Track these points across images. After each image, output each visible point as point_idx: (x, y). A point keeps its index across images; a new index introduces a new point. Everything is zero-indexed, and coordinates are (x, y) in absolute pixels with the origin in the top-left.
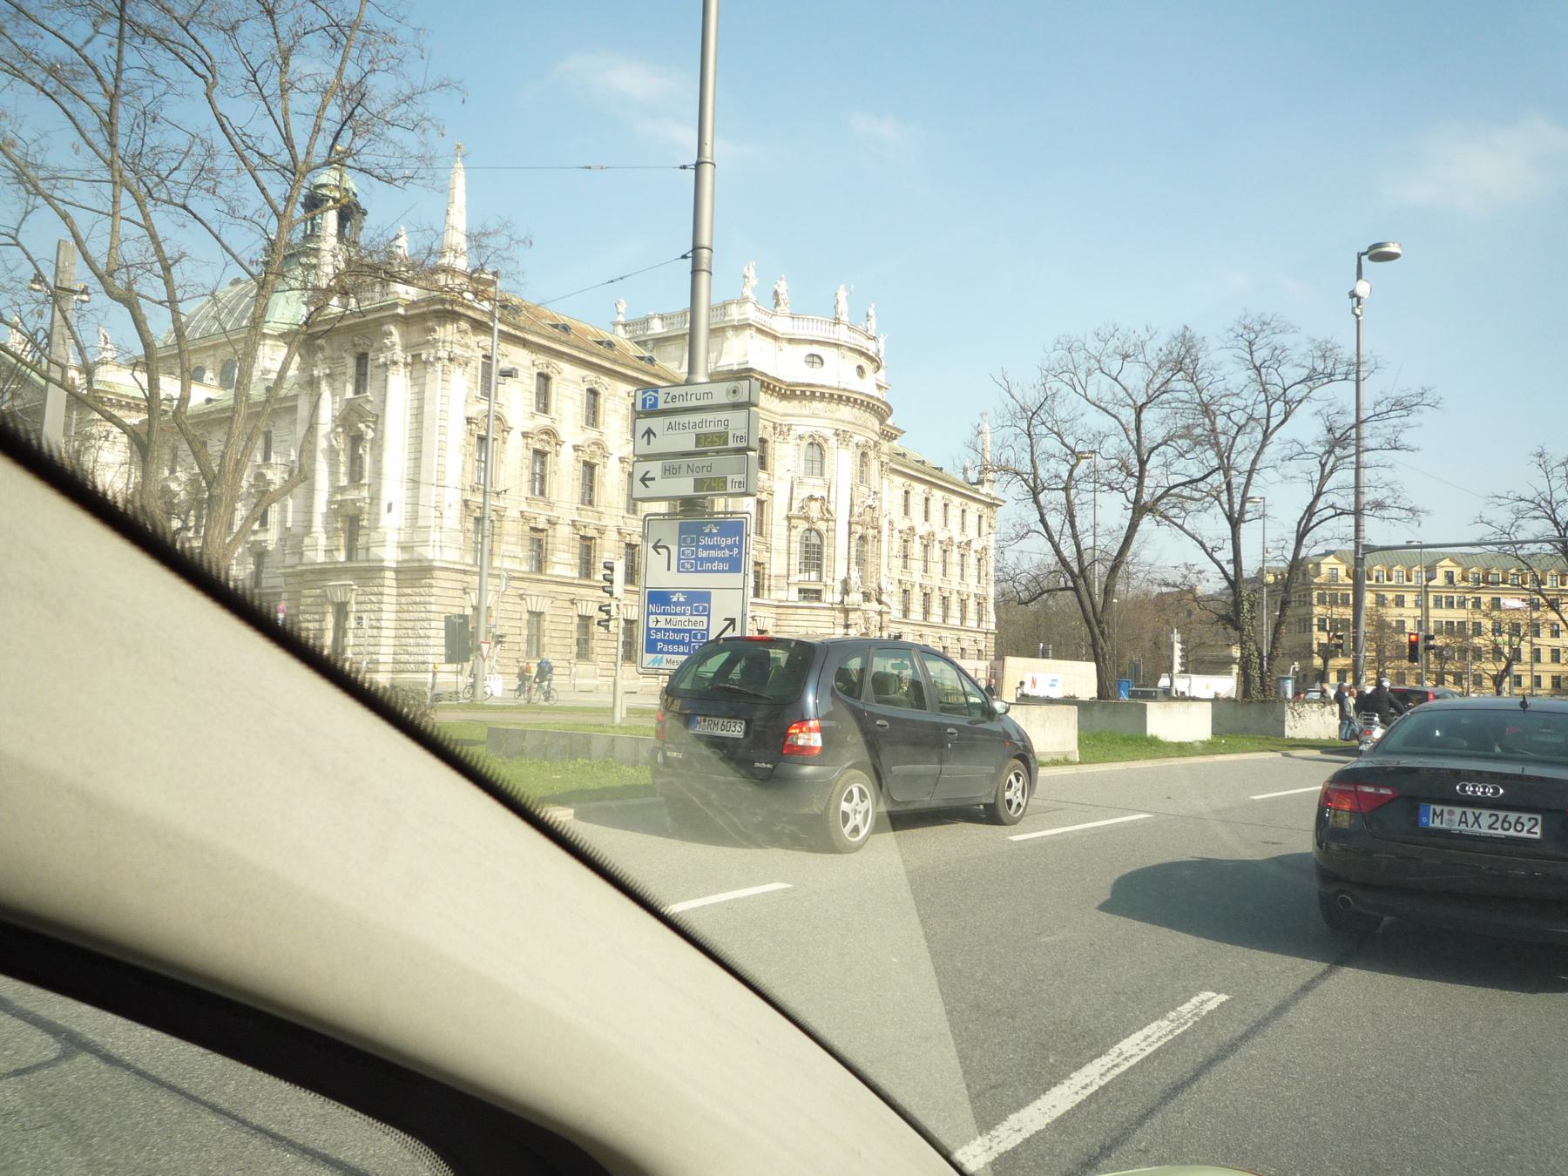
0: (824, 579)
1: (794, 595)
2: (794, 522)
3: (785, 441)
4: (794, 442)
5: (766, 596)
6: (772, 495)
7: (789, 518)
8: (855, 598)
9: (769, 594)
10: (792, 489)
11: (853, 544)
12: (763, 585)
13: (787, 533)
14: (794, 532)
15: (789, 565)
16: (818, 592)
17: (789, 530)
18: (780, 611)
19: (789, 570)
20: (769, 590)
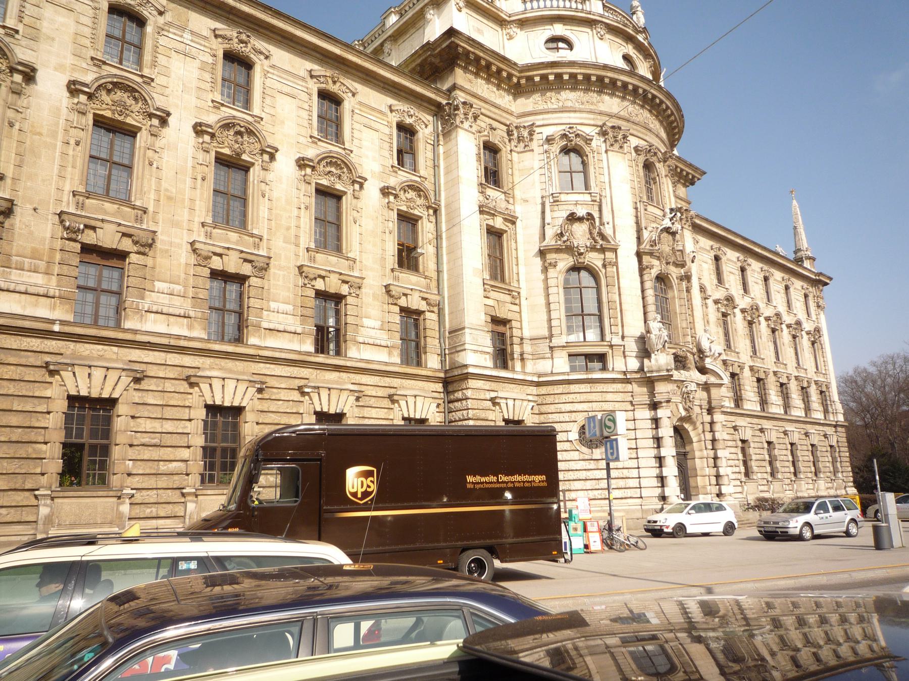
0: (608, 337)
1: (561, 364)
2: (551, 257)
3: (527, 149)
4: (541, 150)
5: (518, 365)
6: (514, 223)
7: (542, 253)
8: (661, 360)
9: (523, 366)
10: (543, 212)
11: (650, 293)
12: (512, 354)
13: (542, 277)
14: (552, 273)
15: (550, 320)
16: (602, 358)
17: (545, 270)
18: (544, 390)
20: (522, 359)
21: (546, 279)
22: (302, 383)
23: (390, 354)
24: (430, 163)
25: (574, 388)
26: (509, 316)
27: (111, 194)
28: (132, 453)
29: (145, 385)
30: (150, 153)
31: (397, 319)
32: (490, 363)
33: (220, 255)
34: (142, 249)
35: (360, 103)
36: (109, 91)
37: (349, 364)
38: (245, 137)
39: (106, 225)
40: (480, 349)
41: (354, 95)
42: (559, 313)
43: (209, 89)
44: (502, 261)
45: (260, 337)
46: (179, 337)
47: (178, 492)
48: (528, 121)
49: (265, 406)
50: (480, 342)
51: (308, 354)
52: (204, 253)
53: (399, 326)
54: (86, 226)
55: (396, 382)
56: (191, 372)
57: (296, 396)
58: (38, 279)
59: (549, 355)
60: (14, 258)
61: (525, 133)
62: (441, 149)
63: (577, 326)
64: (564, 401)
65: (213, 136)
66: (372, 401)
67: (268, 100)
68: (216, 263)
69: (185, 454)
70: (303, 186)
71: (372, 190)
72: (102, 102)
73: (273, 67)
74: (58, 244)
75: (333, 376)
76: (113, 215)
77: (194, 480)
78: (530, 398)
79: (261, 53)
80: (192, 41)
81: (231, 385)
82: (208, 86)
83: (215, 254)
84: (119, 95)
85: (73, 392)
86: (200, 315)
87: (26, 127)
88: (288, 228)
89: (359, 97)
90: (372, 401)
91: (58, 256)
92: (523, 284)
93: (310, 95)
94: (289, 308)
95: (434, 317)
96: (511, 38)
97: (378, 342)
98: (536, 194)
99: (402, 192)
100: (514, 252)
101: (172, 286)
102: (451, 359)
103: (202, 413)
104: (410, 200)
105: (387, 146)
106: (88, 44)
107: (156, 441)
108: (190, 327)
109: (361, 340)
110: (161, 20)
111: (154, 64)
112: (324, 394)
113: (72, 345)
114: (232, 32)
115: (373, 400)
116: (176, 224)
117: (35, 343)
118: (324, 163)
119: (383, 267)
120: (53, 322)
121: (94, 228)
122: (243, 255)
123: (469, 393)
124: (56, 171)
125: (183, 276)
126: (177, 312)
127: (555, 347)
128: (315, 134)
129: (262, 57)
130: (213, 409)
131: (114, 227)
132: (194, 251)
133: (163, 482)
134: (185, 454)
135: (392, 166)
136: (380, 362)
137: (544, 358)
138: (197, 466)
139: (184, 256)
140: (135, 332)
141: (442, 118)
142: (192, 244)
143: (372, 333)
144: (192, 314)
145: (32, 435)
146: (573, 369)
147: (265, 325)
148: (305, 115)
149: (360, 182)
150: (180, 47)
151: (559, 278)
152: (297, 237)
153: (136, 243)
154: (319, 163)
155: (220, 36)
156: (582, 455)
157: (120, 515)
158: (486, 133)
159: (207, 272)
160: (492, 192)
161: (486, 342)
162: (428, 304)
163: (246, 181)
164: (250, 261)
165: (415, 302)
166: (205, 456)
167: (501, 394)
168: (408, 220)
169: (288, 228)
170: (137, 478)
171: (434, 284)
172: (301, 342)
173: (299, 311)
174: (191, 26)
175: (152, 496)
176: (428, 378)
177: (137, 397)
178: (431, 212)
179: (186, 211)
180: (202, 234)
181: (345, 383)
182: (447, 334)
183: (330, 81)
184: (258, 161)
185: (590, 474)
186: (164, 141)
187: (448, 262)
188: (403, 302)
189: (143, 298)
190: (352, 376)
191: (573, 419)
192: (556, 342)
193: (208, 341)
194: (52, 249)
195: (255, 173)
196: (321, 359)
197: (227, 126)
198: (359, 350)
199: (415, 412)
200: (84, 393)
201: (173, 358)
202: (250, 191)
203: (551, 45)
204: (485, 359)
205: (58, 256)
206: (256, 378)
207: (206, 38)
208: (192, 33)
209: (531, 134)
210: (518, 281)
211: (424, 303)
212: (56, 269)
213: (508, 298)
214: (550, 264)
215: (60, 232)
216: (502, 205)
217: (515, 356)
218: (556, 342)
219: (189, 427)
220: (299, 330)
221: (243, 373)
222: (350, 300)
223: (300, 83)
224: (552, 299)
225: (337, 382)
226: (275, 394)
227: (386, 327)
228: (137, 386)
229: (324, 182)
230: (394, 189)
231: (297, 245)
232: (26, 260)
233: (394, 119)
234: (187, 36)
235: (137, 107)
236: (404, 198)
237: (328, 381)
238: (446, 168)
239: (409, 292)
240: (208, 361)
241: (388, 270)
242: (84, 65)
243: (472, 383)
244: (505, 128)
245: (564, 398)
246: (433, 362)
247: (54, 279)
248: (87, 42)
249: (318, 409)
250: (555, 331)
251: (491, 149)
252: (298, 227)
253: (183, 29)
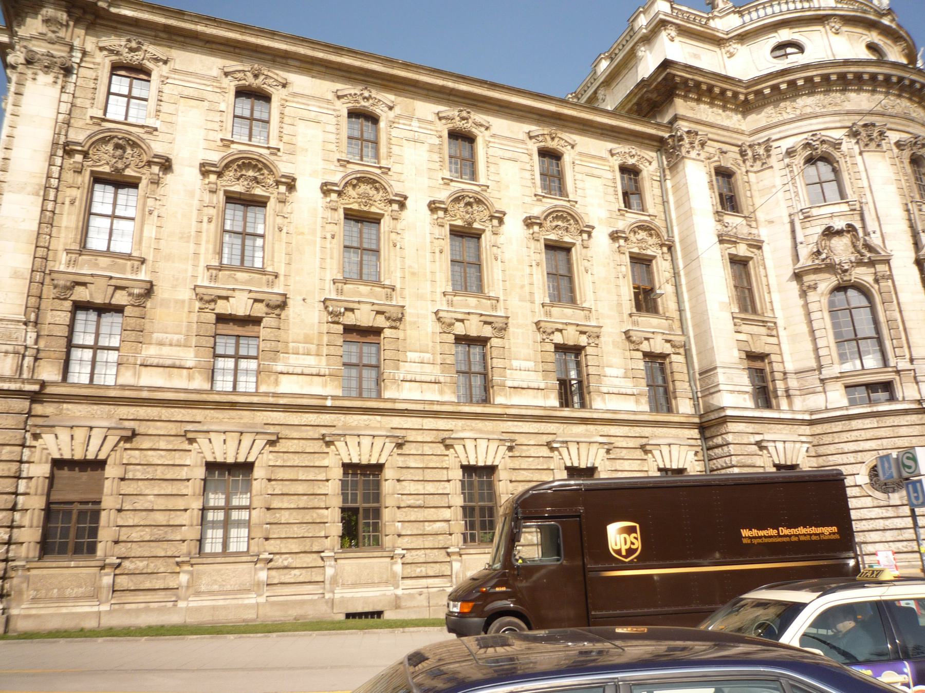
0: (892, 362)
1: (837, 398)
2: (809, 279)
3: (766, 167)
4: (782, 165)
6: (760, 248)
7: (798, 276)
9: (790, 404)
10: (793, 231)
12: (775, 391)
13: (802, 302)
14: (812, 296)
15: (816, 349)
16: (887, 386)
17: (804, 294)
18: (818, 429)
19: (818, 358)
20: (788, 396)
21: (806, 305)
22: (550, 438)
23: (637, 402)
24: (659, 200)
25: (856, 424)
26: (767, 350)
27: (365, 277)
28: (401, 515)
29: (406, 449)
30: (393, 236)
31: (641, 365)
32: (750, 403)
33: (462, 321)
34: (394, 324)
35: (580, 154)
36: (354, 186)
37: (595, 416)
38: (475, 207)
39: (362, 306)
40: (737, 388)
41: (573, 147)
42: (827, 340)
43: (439, 168)
44: (750, 290)
45: (505, 395)
46: (432, 402)
47: (443, 551)
48: (762, 137)
49: (516, 463)
50: (736, 380)
51: (553, 408)
52: (448, 321)
53: (644, 372)
54: (346, 309)
55: (647, 431)
56: (446, 435)
57: (545, 451)
58: (311, 360)
59: (821, 389)
60: (291, 345)
61: (761, 151)
62: (669, 184)
63: (852, 353)
64: (846, 440)
65: (446, 210)
66: (624, 454)
67: (492, 168)
68: (459, 329)
69: (447, 514)
70: (533, 244)
71: (601, 237)
72: (350, 197)
73: (493, 136)
74: (325, 328)
75: (580, 429)
76: (367, 296)
77: (458, 539)
78: (803, 439)
79: (481, 125)
80: (420, 127)
81: (482, 444)
82: (437, 166)
83: (458, 320)
84: (364, 188)
85: (347, 461)
86: (448, 380)
87: (291, 230)
88: (522, 287)
89: (577, 148)
90: (624, 454)
91: (325, 339)
92: (779, 313)
93: (530, 155)
94: (531, 365)
95: (681, 359)
96: (731, 55)
97: (623, 391)
98: (783, 215)
99: (632, 234)
100: (764, 279)
101: (422, 355)
102: (704, 402)
103: (458, 474)
104: (641, 241)
105: (611, 190)
106: (335, 149)
107: (420, 503)
108: (441, 392)
109: (605, 390)
110: (391, 114)
111: (389, 155)
112: (573, 448)
113: (342, 417)
114: (453, 112)
115: (624, 451)
116: (420, 297)
117: (312, 418)
118: (550, 218)
119: (621, 313)
120: (325, 398)
121: (352, 310)
122: (483, 318)
123: (730, 438)
124: (318, 264)
125: (431, 344)
126: (428, 379)
127: (826, 379)
128: (539, 192)
129: (483, 129)
130: (468, 469)
131: (369, 307)
132: (439, 319)
133: (429, 542)
134: (447, 514)
135: (619, 210)
136: (627, 412)
138: (459, 526)
139: (431, 326)
140: (394, 400)
141: (666, 151)
142: (436, 313)
143: (616, 382)
144: (442, 379)
145: (316, 502)
146: (853, 403)
147: (509, 383)
148: (527, 175)
149: (588, 231)
150: (410, 135)
151: (823, 301)
152: (531, 293)
153: (388, 319)
154: (545, 219)
155: (444, 118)
157: (394, 575)
158: (716, 158)
159: (451, 338)
160: (733, 220)
161: (744, 381)
162: (673, 346)
163: (478, 248)
164: (490, 323)
165: (658, 346)
166: (465, 516)
167: (767, 437)
168: (641, 262)
169: (522, 287)
170: (406, 539)
171: (676, 325)
172: (546, 397)
173: (540, 367)
174: (418, 114)
175: (420, 556)
176: (681, 425)
177: (400, 461)
178: (665, 249)
179: (429, 283)
180: (445, 303)
181: (593, 436)
182: (697, 376)
183: (548, 138)
184: (488, 227)
185: (889, 523)
186: (404, 223)
187: (690, 300)
188: (645, 347)
189: (398, 369)
190: (599, 428)
191: (859, 460)
192: (826, 373)
193: (458, 403)
194: (320, 333)
195: (486, 238)
196: (566, 412)
197: (457, 200)
198: (604, 400)
199: (671, 462)
200: (355, 460)
201: (429, 423)
202: (484, 256)
203: (778, 53)
204: (745, 399)
205: (325, 339)
206: (505, 436)
207: (431, 122)
208: (419, 120)
209: (768, 150)
210: (773, 310)
211: (668, 345)
212: (325, 350)
213: (763, 330)
214: (809, 287)
215: (326, 317)
216: (744, 231)
217: (779, 393)
218: (826, 373)
219: (448, 488)
220: (542, 386)
221: (493, 433)
222: (589, 350)
223: (520, 146)
224: (816, 325)
225: (585, 436)
226: (525, 451)
227: (630, 374)
228: (400, 451)
229: (553, 237)
230: (624, 232)
231: (533, 302)
232: (301, 345)
233: (616, 162)
234: (415, 124)
235: (378, 196)
236: (635, 240)
237: (577, 435)
238: (676, 202)
239: (650, 335)
240: (460, 423)
241: (626, 316)
242: (333, 168)
243: (732, 427)
244: (737, 149)
245: (845, 437)
246: (685, 407)
247: (324, 359)
248: (333, 147)
249: (569, 464)
250: (824, 361)
251: (724, 174)
252: (531, 284)
253: (411, 118)
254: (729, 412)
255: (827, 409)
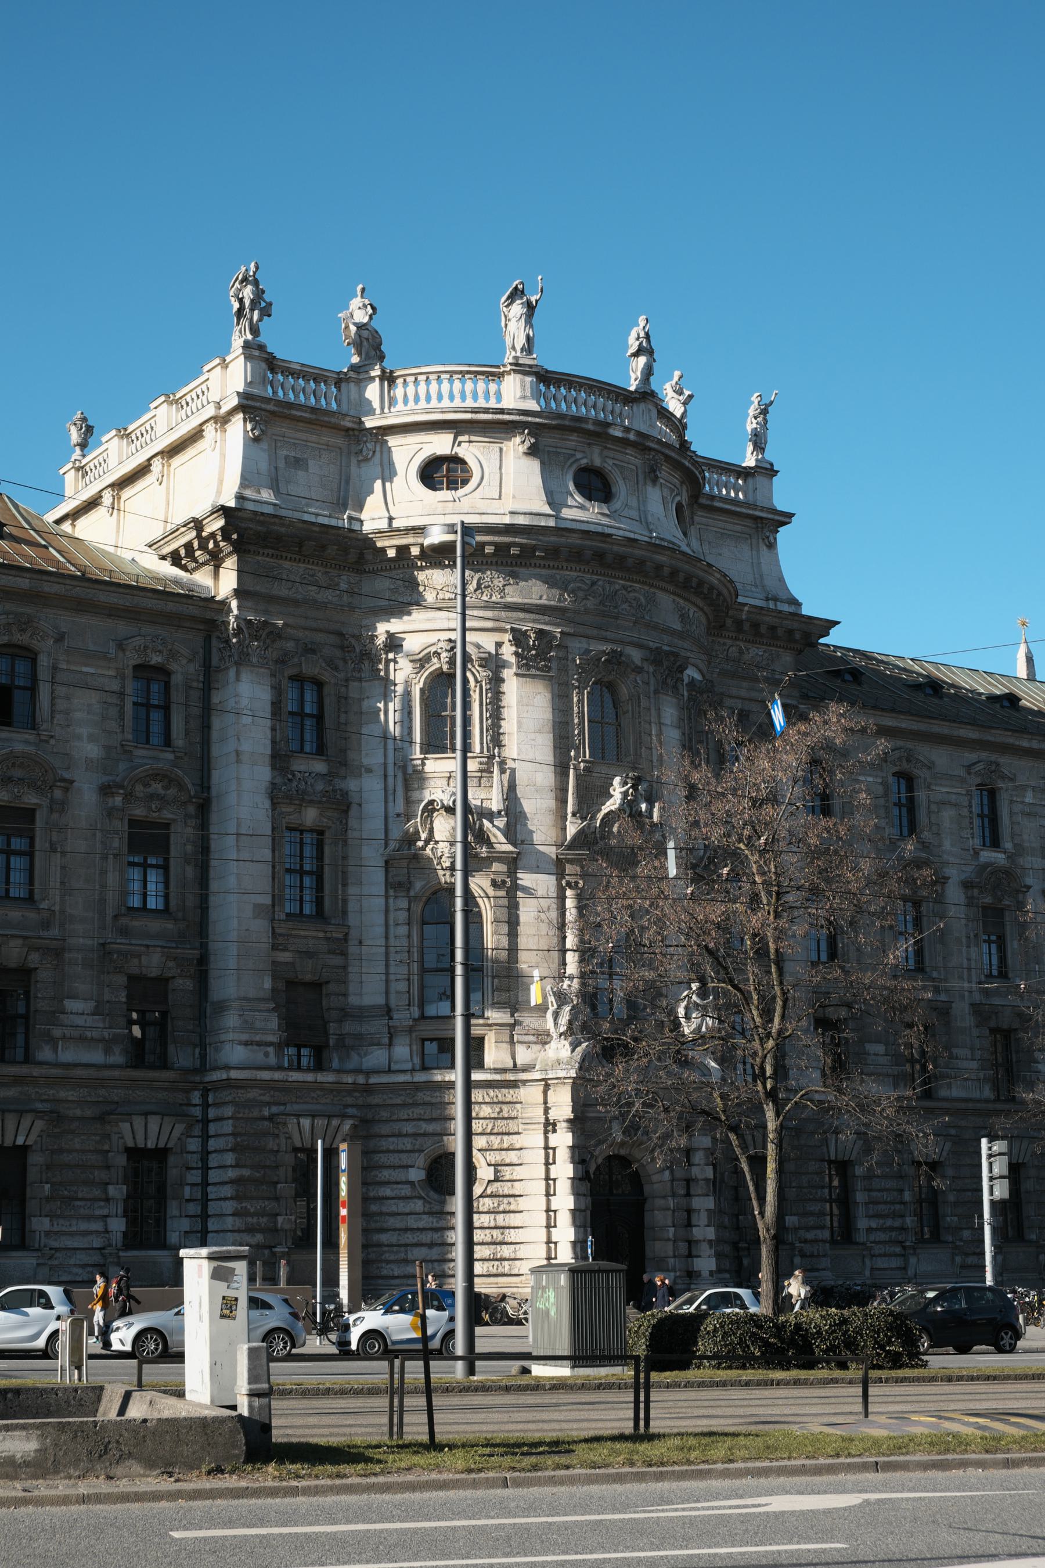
23: (107, 1051)
40: (257, 1038)
59: (386, 1040)
64: (406, 1117)
78: (350, 1111)
95: (188, 984)
137: (379, 1044)
156: (428, 1206)
161: (270, 1026)
167: (289, 1108)
188: (133, 966)
198: (56, 1051)
204: (267, 1055)
241: (109, 919)
245: (403, 1114)
254: (234, 1074)
255: (390, 1071)
